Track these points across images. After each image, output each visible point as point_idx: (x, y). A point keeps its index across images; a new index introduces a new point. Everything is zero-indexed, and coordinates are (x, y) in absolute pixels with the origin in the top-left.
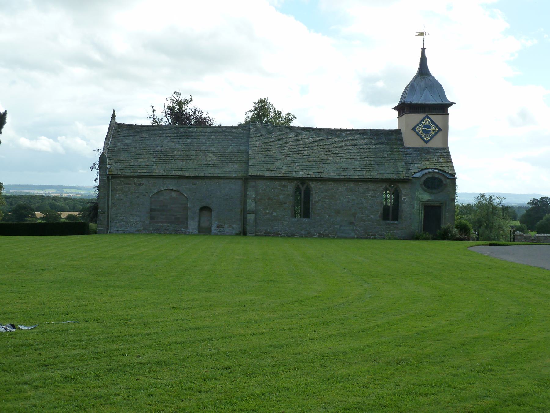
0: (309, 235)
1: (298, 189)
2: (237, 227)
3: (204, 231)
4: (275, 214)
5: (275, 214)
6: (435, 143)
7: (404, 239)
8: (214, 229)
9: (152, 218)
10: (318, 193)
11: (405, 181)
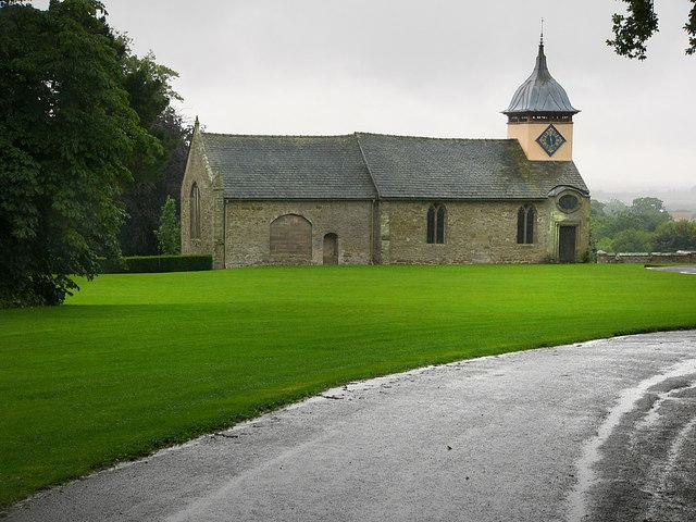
0: (443, 262)
1: (431, 211)
2: (366, 255)
3: (331, 261)
4: (408, 240)
5: (408, 240)
6: (558, 157)
7: (541, 263)
8: (341, 259)
9: (271, 248)
10: (453, 216)
11: (540, 201)
